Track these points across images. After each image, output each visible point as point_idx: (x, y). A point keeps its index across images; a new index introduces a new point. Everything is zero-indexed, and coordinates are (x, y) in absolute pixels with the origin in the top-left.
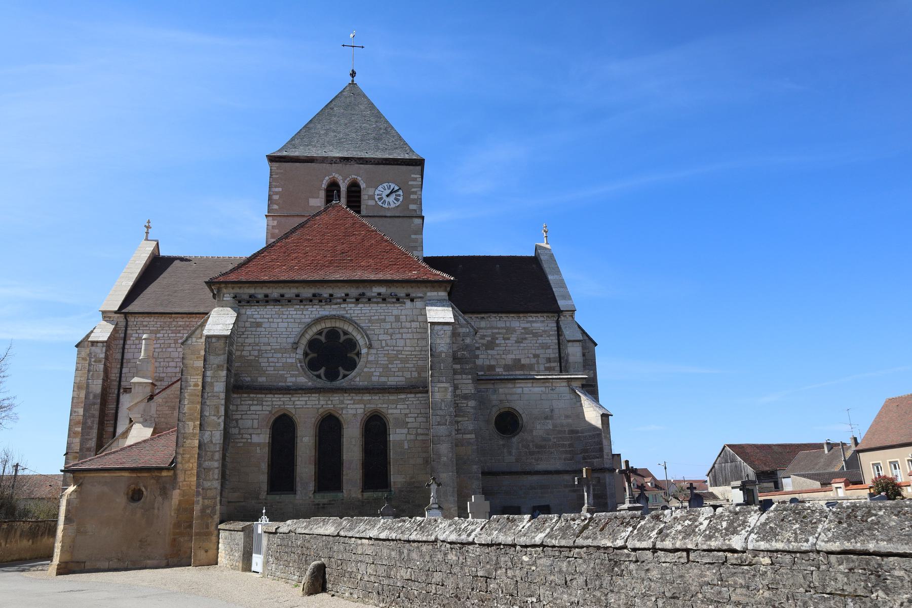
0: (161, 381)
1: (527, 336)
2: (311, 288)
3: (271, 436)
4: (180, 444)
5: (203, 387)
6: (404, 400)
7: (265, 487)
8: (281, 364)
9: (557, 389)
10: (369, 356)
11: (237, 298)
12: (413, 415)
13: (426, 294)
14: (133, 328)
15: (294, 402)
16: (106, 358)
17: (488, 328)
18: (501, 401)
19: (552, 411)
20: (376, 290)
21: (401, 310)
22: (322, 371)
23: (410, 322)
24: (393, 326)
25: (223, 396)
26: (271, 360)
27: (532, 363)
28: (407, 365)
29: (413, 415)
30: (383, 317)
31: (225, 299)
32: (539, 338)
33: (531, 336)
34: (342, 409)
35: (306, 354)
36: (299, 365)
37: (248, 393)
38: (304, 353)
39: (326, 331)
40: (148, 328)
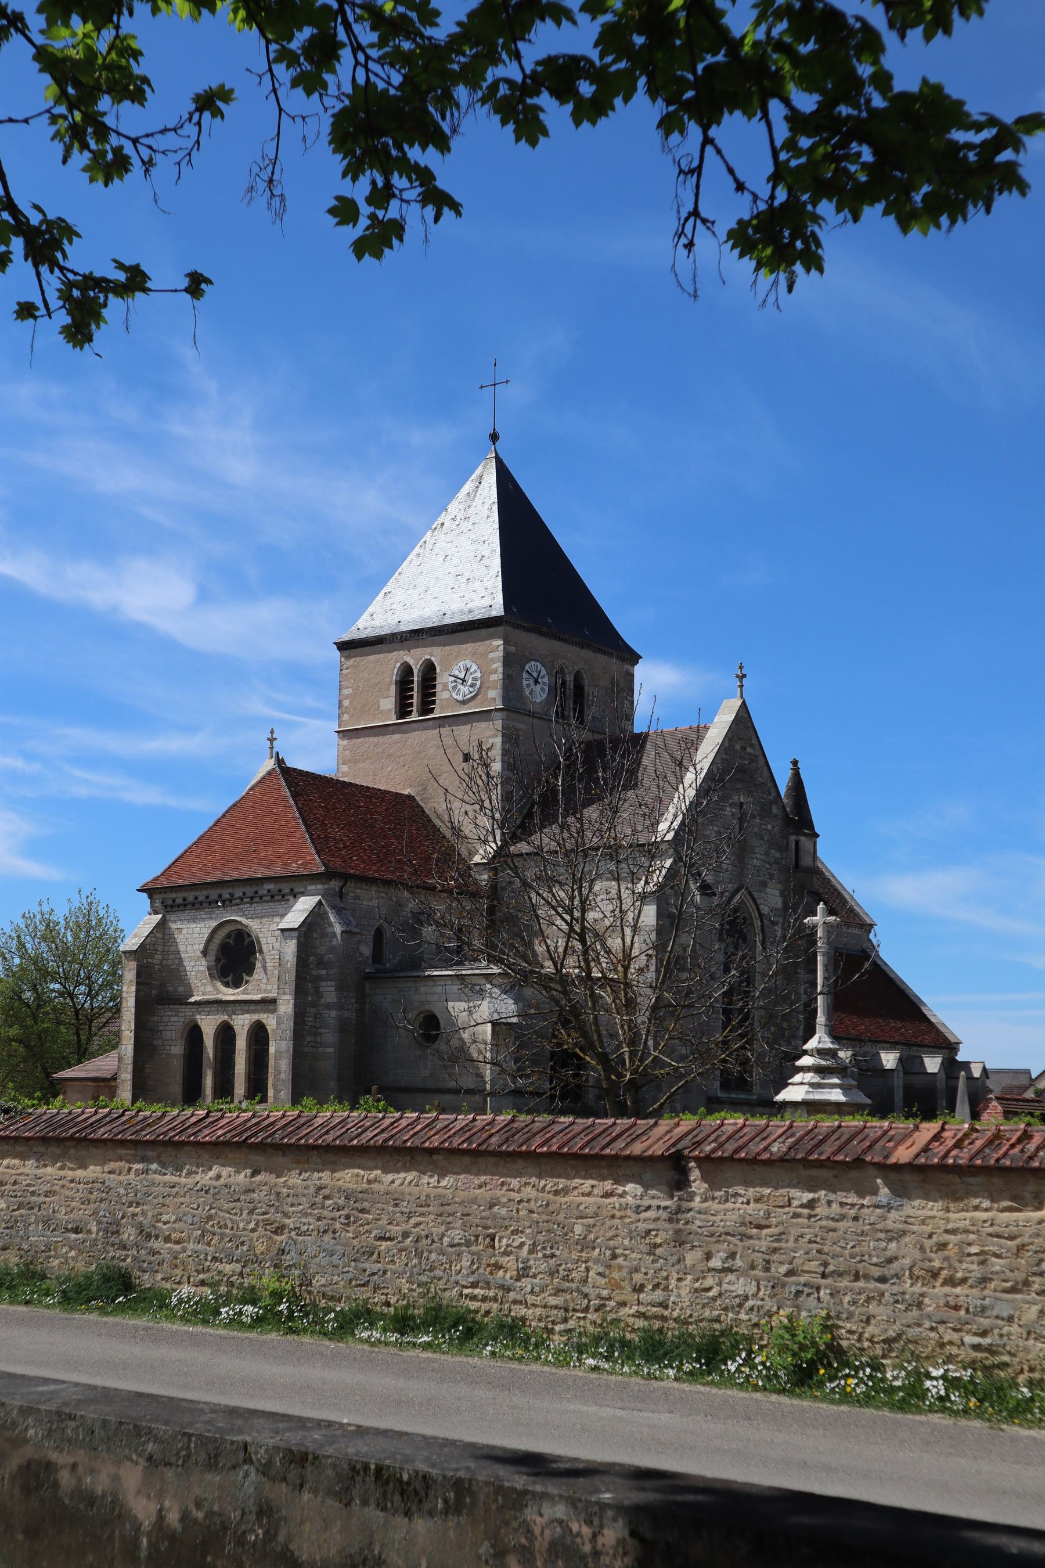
25: (133, 1010)
35: (218, 960)
37: (169, 1004)
39: (234, 934)
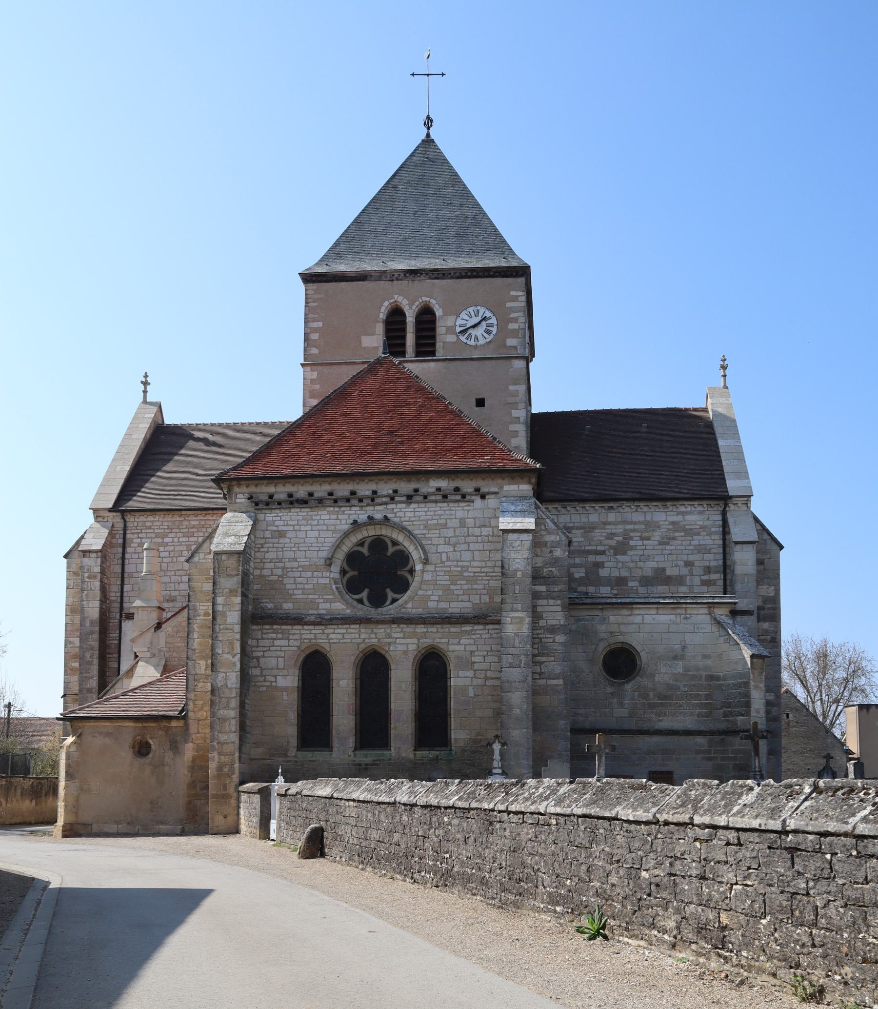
0: (173, 601)
1: (676, 534)
2: (348, 483)
3: (300, 678)
4: (191, 687)
5: (214, 618)
6: (469, 633)
7: (294, 742)
8: (310, 586)
9: (693, 618)
10: (425, 574)
11: (253, 500)
12: (481, 653)
13: (502, 488)
14: (133, 531)
15: (328, 635)
16: (103, 572)
17: (618, 523)
18: (611, 633)
19: (684, 648)
20: (435, 483)
21: (468, 511)
22: (364, 595)
23: (480, 527)
24: (457, 534)
25: (237, 628)
26: (298, 580)
27: (681, 574)
28: (475, 586)
29: (481, 653)
30: (443, 521)
31: (238, 501)
32: (695, 537)
33: (683, 534)
34: (389, 644)
35: (343, 572)
36: (334, 587)
37: (272, 624)
38: (341, 571)
39: (369, 540)
40: (152, 531)
